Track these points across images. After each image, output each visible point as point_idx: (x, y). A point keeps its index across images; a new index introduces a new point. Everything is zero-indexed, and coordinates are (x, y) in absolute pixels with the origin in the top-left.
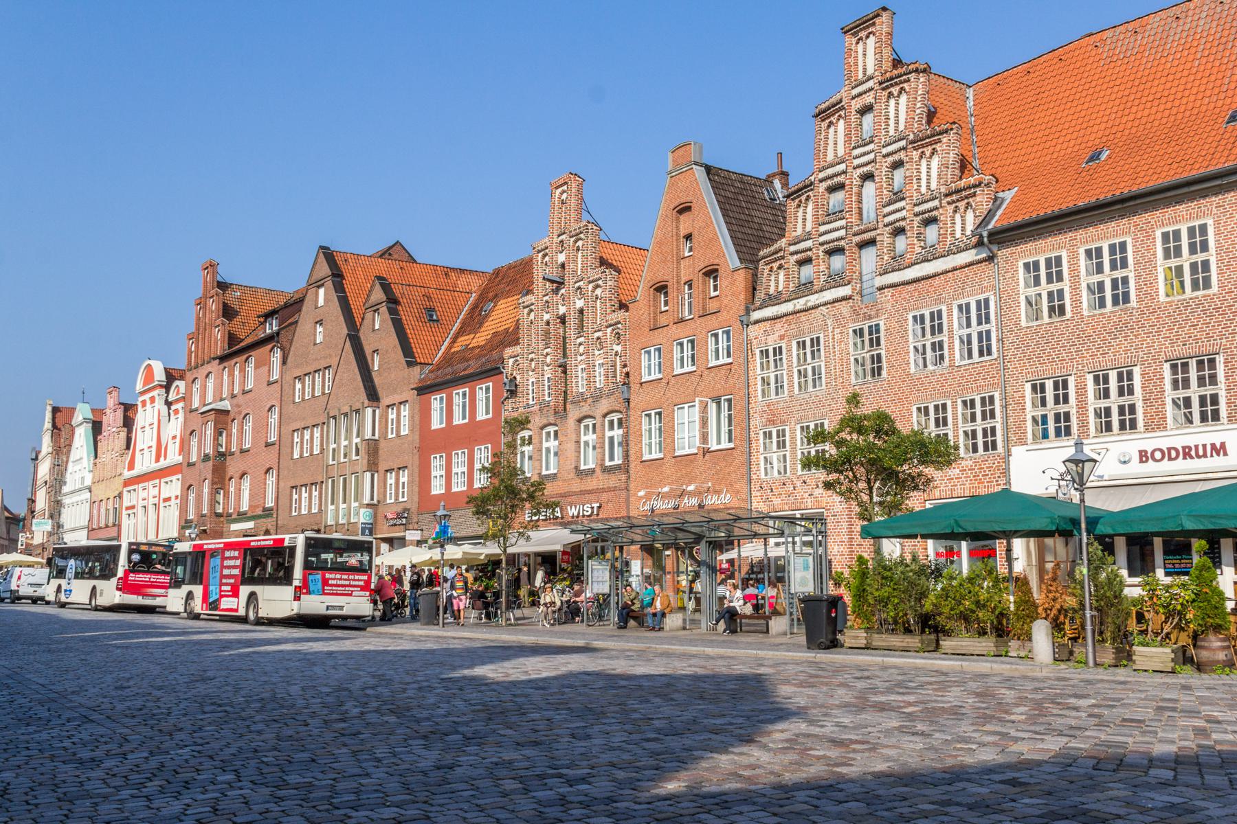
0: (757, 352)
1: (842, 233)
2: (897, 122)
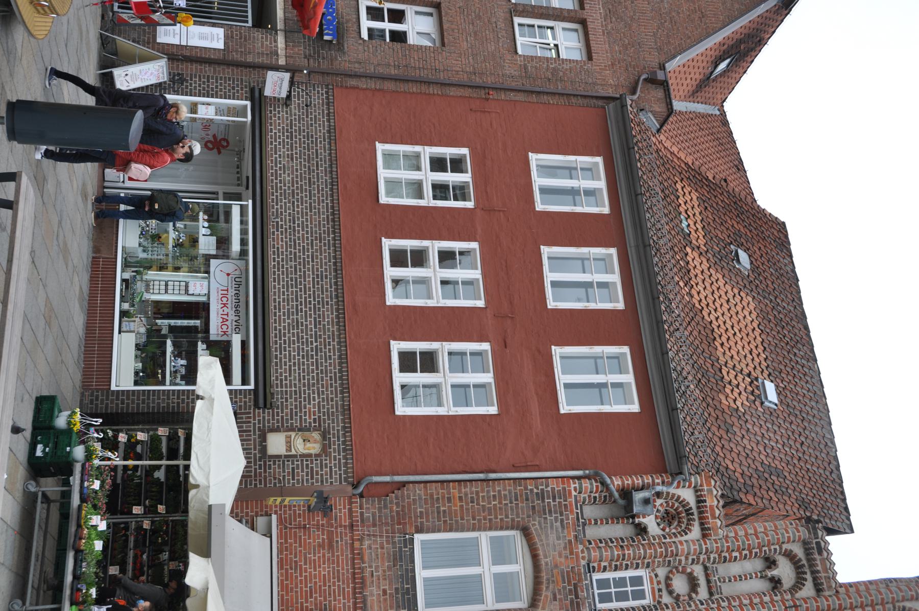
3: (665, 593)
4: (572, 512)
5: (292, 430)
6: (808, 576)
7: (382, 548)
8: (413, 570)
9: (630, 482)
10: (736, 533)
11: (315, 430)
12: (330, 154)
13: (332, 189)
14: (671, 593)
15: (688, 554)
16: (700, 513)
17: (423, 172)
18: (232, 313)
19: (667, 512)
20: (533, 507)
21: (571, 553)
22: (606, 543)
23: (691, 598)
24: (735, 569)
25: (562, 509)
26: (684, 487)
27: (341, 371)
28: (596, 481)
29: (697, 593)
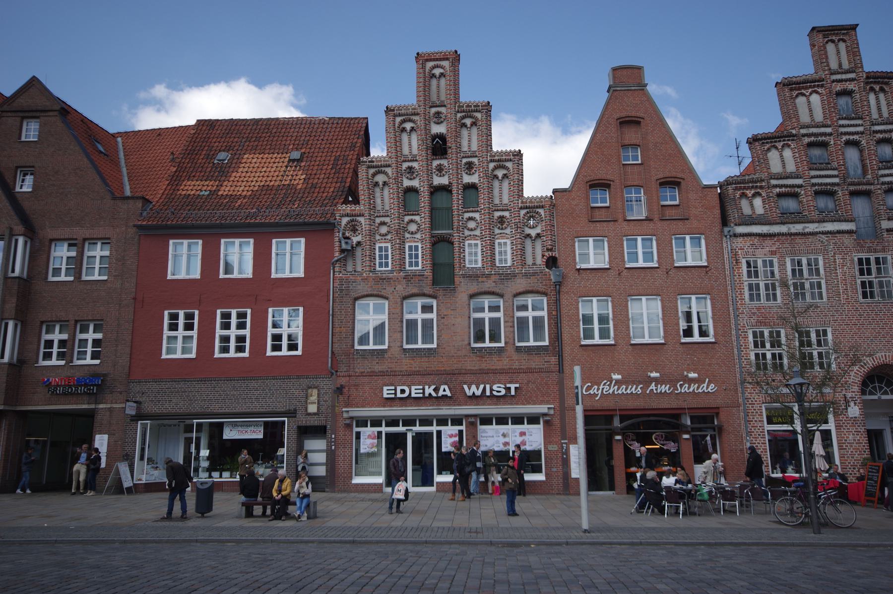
0: (744, 261)
1: (836, 180)
2: (879, 109)
3: (386, 237)
4: (349, 277)
5: (307, 401)
6: (383, 169)
7: (359, 363)
8: (370, 350)
9: (337, 248)
10: (363, 200)
11: (307, 391)
12: (168, 382)
13: (188, 381)
14: (386, 235)
15: (370, 225)
16: (353, 216)
17: (179, 335)
18: (250, 428)
19: (352, 230)
20: (346, 294)
21: (366, 279)
22: (363, 262)
23: (389, 226)
24: (378, 201)
25: (348, 281)
26: (340, 222)
27: (281, 379)
28: (336, 264)
29: (387, 223)
